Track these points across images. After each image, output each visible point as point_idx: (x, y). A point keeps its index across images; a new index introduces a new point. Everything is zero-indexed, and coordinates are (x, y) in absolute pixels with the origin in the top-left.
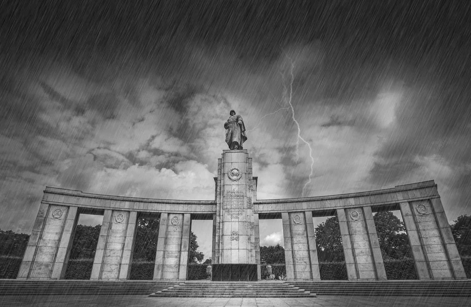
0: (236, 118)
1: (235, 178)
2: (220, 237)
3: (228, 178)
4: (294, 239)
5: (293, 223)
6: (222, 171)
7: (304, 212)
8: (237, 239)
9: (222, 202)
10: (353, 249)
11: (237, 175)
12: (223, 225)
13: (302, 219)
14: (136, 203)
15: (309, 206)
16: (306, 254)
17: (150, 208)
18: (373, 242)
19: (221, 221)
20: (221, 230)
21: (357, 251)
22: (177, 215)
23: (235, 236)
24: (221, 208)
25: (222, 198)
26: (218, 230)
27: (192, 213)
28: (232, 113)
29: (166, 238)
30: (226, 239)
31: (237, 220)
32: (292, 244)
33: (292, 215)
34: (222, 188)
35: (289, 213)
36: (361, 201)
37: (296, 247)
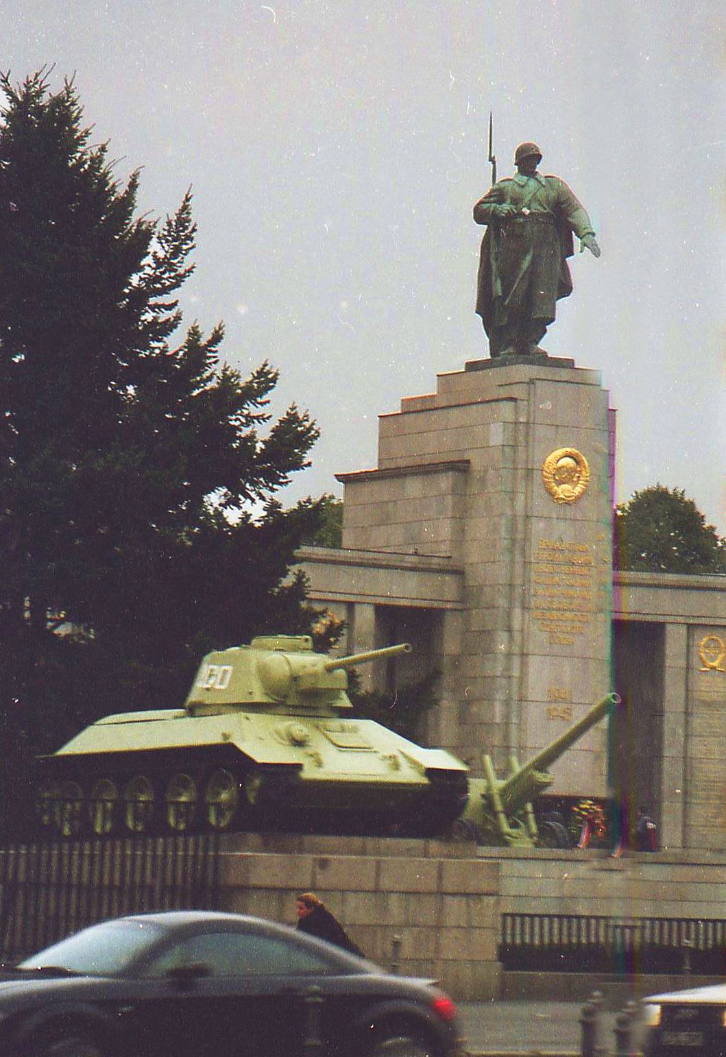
0: (553, 194)
1: (564, 490)
2: (514, 705)
3: (543, 492)
4: (696, 722)
6: (521, 455)
9: (518, 581)
11: (569, 480)
12: (524, 665)
19: (516, 649)
20: (515, 681)
24: (517, 604)
25: (518, 569)
26: (504, 681)
27: (382, 601)
28: (528, 159)
33: (697, 633)
34: (520, 527)
37: (697, 748)
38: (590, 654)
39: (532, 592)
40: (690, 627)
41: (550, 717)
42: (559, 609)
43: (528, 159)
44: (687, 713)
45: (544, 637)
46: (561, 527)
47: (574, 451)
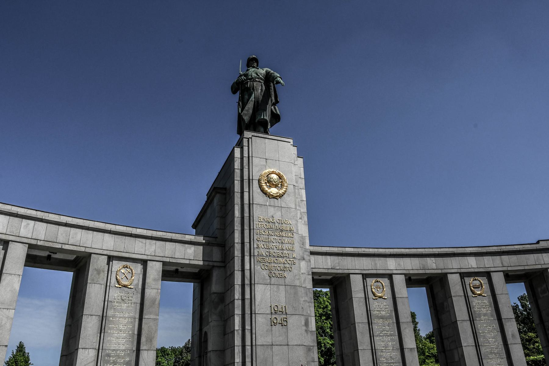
1: (274, 191)
3: (259, 190)
4: (375, 327)
5: (371, 295)
7: (390, 276)
8: (284, 324)
10: (477, 346)
13: (387, 289)
14: (25, 222)
15: (399, 265)
16: (397, 355)
17: (61, 239)
18: (510, 333)
21: (483, 350)
22: (128, 264)
23: (279, 318)
24: (247, 254)
27: (168, 260)
29: (103, 318)
30: (261, 322)
31: (281, 281)
32: (371, 336)
35: (365, 276)
36: (488, 263)
37: (379, 344)
38: (297, 283)
39: (255, 246)
40: (363, 275)
41: (273, 324)
42: (274, 257)
43: (252, 62)
44: (370, 323)
45: (265, 273)
46: (271, 211)
47: (277, 171)
